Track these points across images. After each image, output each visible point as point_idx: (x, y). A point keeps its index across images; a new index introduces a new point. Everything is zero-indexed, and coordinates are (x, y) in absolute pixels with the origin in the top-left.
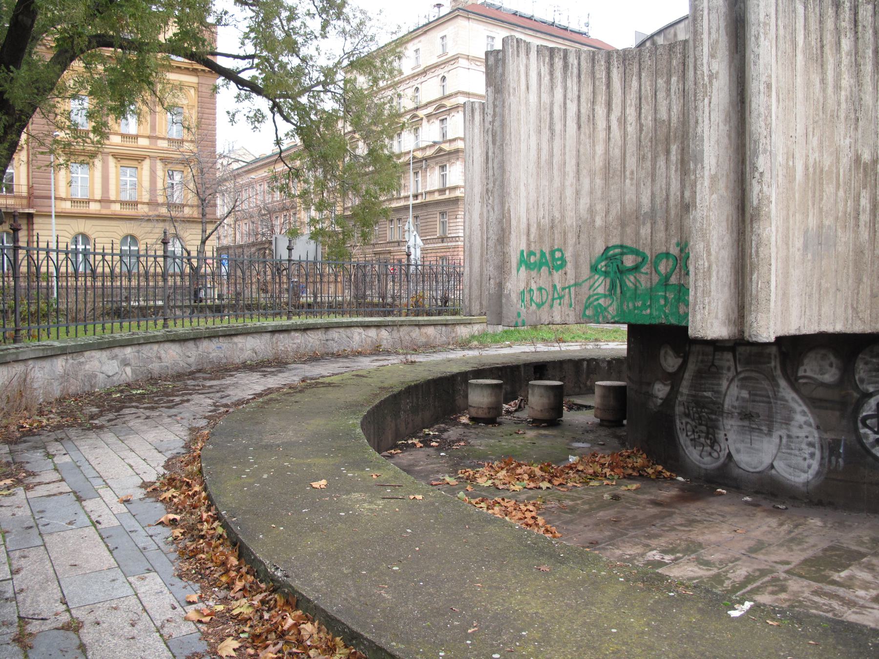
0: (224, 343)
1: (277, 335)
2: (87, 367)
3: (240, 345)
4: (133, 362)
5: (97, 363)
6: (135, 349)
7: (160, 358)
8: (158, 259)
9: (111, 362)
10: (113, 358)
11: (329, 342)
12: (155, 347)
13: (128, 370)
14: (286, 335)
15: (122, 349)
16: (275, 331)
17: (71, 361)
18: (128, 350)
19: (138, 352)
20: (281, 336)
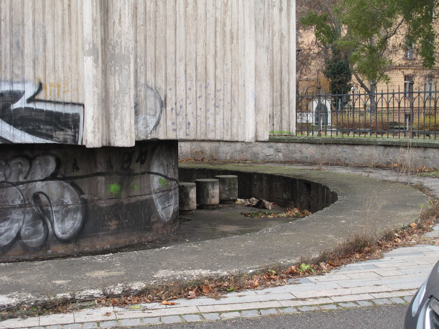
0: (347, 149)
1: (388, 149)
2: (254, 149)
3: (360, 152)
4: (282, 151)
5: (260, 148)
6: (284, 144)
7: (301, 151)
8: (361, 96)
9: (268, 149)
10: (270, 147)
11: (426, 159)
12: (298, 145)
13: (280, 154)
14: (396, 150)
15: (275, 144)
16: (386, 145)
17: (245, 145)
18: (280, 144)
19: (288, 146)
20: (392, 150)
